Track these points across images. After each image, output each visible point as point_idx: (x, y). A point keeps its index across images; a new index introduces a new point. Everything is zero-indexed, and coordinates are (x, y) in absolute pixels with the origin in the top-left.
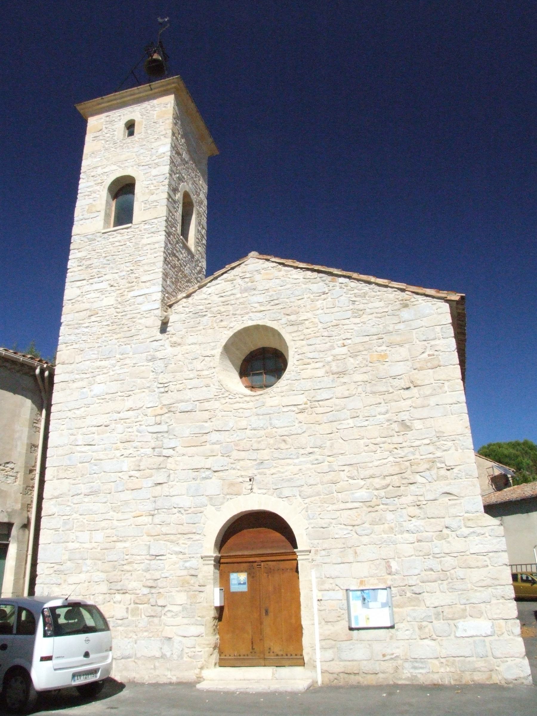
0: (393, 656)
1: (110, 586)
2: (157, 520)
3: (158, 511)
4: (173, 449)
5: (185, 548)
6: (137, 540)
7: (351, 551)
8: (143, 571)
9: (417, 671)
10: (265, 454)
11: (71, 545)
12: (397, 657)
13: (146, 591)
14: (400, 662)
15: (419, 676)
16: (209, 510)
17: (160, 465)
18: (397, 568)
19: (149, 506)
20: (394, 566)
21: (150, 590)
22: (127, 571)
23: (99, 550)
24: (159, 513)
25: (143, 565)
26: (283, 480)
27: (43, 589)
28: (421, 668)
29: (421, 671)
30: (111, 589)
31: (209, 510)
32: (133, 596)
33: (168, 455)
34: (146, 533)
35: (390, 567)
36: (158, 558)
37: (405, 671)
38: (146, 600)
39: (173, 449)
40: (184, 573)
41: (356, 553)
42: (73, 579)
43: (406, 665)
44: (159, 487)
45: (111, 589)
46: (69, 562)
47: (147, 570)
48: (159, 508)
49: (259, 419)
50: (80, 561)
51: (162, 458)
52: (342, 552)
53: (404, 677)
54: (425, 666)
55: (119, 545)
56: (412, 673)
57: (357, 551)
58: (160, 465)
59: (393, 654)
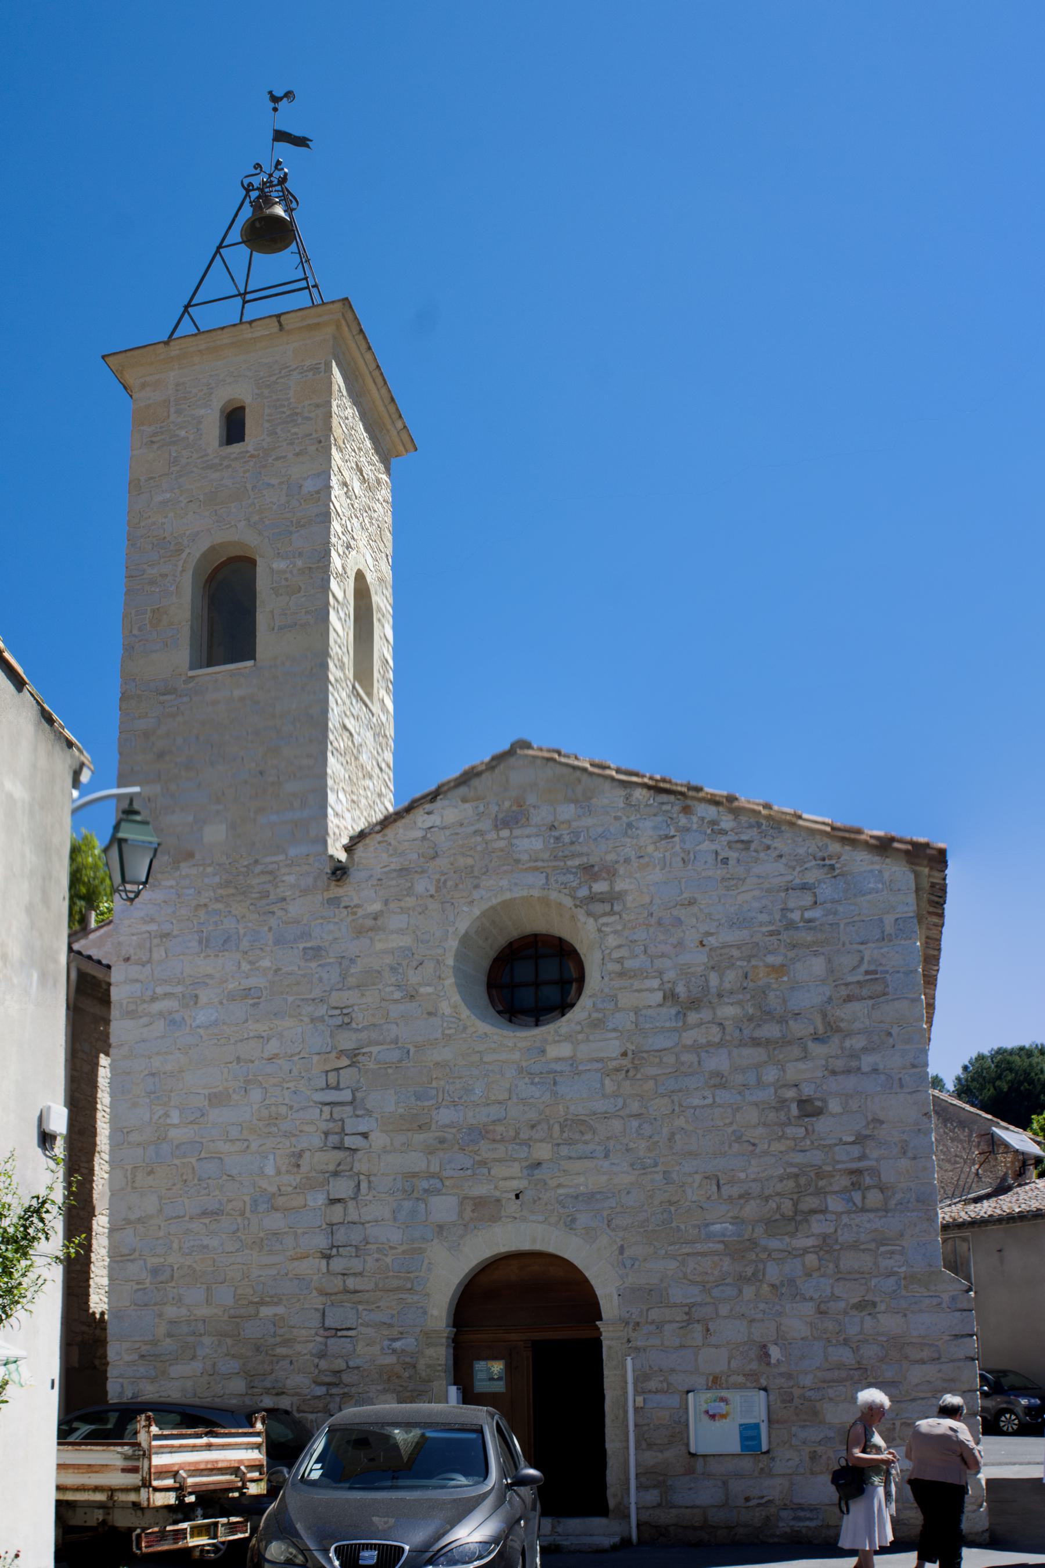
0: (763, 1501)
1: (251, 1381)
2: (337, 1265)
3: (338, 1251)
4: (365, 1135)
5: (393, 1316)
6: (299, 1300)
7: (698, 1327)
8: (312, 1355)
9: (801, 1524)
10: (543, 1151)
11: (171, 1312)
12: (769, 1501)
13: (320, 1391)
14: (773, 1510)
15: (804, 1531)
16: (437, 1253)
17: (339, 1164)
18: (781, 1358)
19: (321, 1242)
20: (775, 1353)
21: (327, 1391)
22: (283, 1356)
23: (226, 1318)
24: (338, 1254)
25: (312, 1345)
26: (576, 1197)
27: (122, 1386)
28: (811, 1519)
29: (807, 1523)
30: (253, 1387)
31: (437, 1253)
32: (295, 1399)
33: (354, 1147)
34: (316, 1289)
35: (767, 1355)
36: (340, 1333)
37: (781, 1524)
38: (321, 1405)
39: (365, 1135)
40: (391, 1360)
41: (708, 1330)
42: (176, 1370)
43: (784, 1514)
44: (338, 1208)
45: (253, 1387)
46: (168, 1340)
47: (322, 1355)
48: (340, 1244)
49: (532, 1083)
50: (191, 1339)
51: (340, 1155)
52: (682, 1328)
53: (778, 1533)
54: (815, 1517)
55: (266, 1311)
56: (793, 1526)
57: (710, 1326)
58: (339, 1164)
59: (763, 1497)
